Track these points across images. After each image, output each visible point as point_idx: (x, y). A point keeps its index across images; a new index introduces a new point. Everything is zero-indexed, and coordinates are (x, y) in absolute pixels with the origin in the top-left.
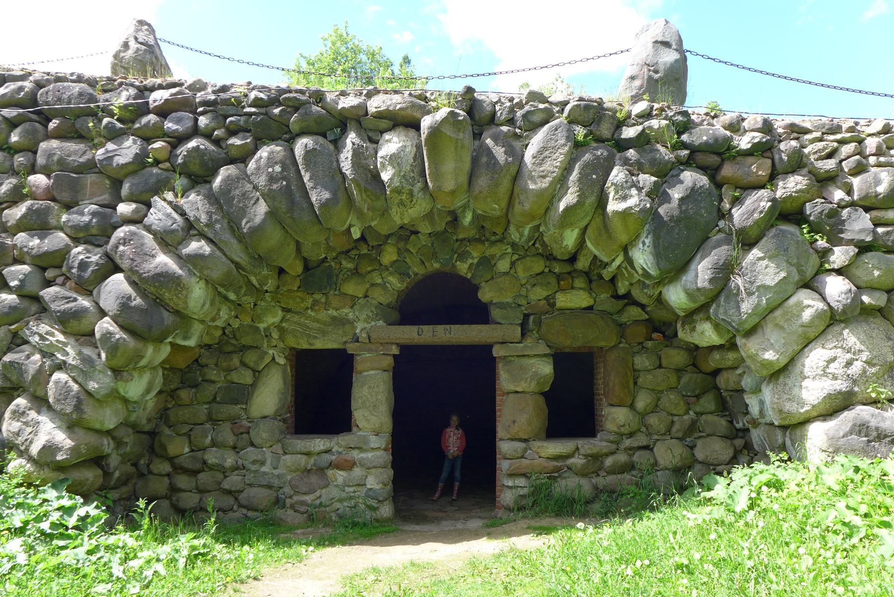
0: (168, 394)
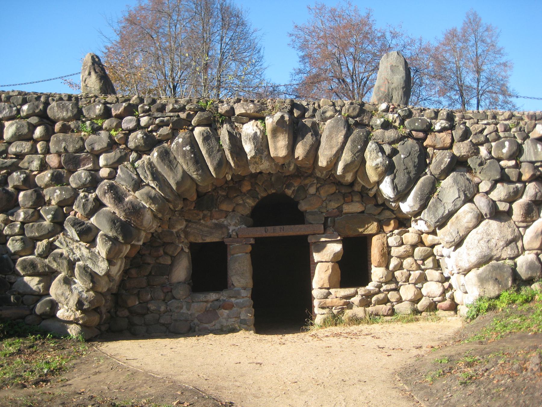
0: (126, 272)
